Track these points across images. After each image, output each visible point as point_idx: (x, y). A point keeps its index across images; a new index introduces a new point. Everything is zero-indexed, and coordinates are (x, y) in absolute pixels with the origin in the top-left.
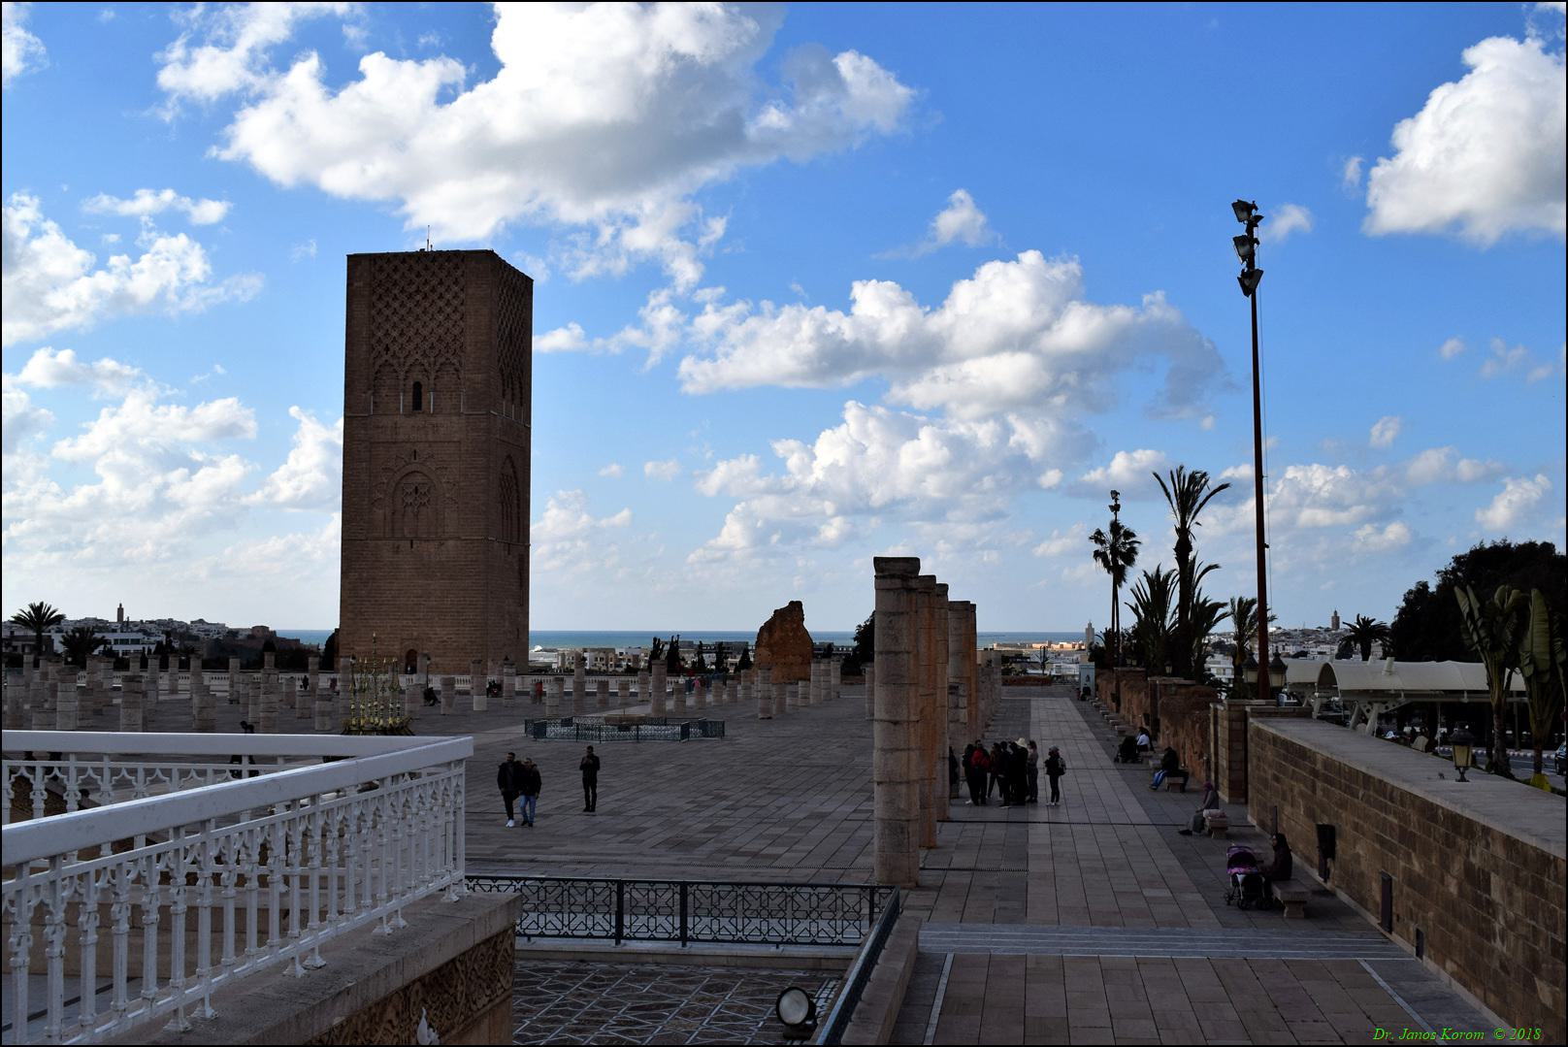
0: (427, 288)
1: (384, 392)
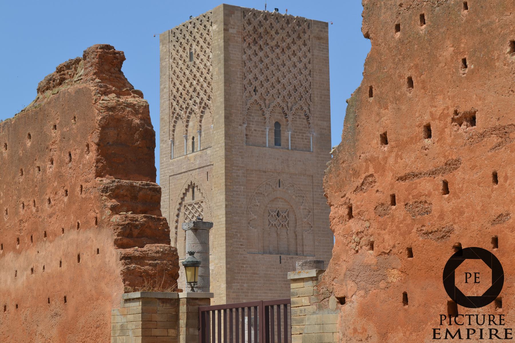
0: (284, 45)
1: (253, 127)
